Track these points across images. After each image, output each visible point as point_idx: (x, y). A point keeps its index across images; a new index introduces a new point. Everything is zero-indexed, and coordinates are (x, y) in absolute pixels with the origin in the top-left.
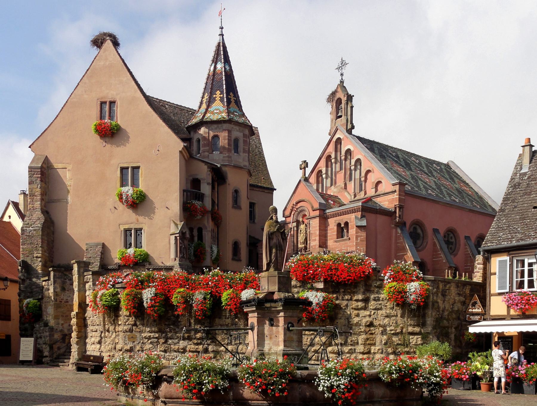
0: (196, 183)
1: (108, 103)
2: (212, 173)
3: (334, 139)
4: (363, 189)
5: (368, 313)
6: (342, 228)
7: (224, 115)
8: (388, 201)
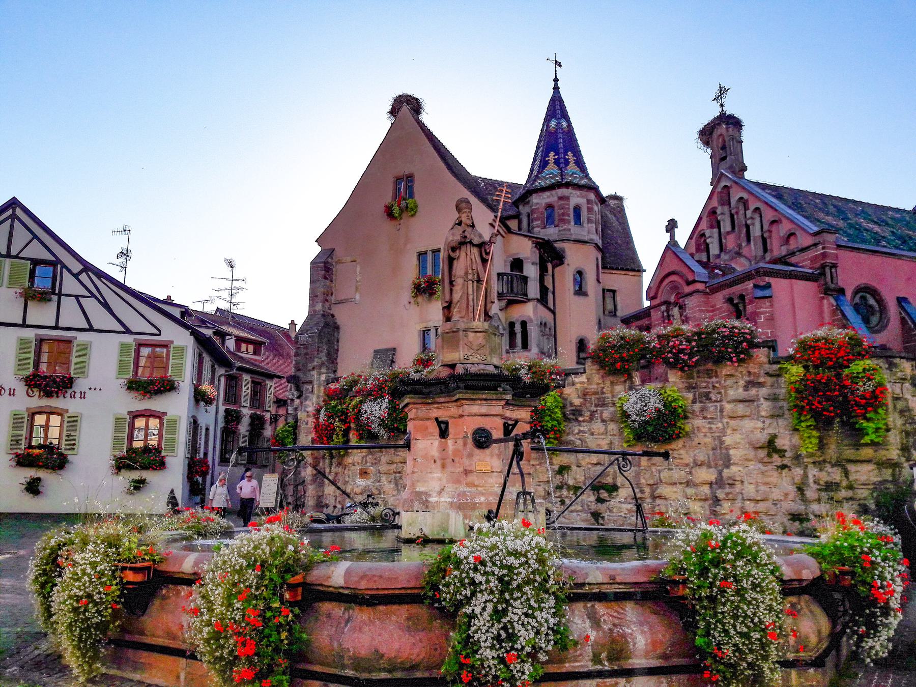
0: (517, 264)
1: (405, 178)
2: (539, 250)
3: (719, 189)
4: (769, 248)
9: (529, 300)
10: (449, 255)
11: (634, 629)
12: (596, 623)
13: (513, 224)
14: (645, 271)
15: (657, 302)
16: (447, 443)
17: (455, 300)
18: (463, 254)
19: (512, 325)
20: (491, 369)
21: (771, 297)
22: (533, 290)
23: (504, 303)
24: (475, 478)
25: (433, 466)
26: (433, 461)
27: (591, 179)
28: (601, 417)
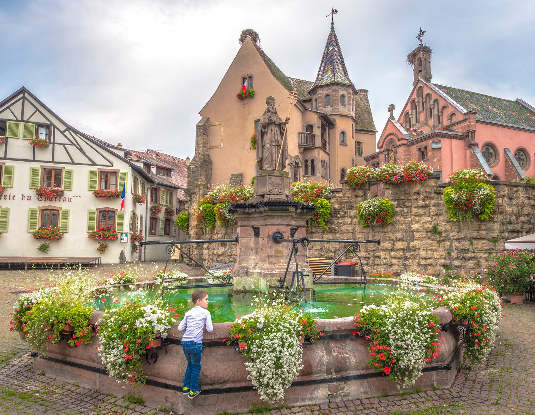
0: (310, 127)
5: (430, 219)
6: (423, 152)
7: (333, 80)
8: (461, 128)
9: (316, 148)
10: (262, 131)
11: (350, 354)
12: (329, 353)
13: (308, 106)
14: (377, 132)
15: (383, 149)
16: (258, 239)
17: (265, 158)
18: (270, 131)
19: (306, 161)
20: (284, 198)
21: (440, 148)
22: (318, 142)
23: (302, 149)
24: (274, 259)
25: (251, 252)
26: (251, 250)
27: (350, 81)
28: (349, 215)
